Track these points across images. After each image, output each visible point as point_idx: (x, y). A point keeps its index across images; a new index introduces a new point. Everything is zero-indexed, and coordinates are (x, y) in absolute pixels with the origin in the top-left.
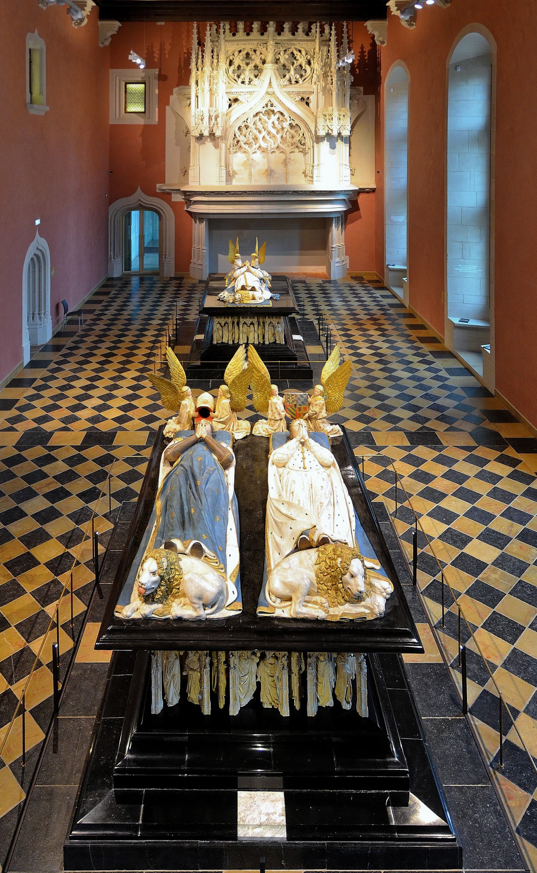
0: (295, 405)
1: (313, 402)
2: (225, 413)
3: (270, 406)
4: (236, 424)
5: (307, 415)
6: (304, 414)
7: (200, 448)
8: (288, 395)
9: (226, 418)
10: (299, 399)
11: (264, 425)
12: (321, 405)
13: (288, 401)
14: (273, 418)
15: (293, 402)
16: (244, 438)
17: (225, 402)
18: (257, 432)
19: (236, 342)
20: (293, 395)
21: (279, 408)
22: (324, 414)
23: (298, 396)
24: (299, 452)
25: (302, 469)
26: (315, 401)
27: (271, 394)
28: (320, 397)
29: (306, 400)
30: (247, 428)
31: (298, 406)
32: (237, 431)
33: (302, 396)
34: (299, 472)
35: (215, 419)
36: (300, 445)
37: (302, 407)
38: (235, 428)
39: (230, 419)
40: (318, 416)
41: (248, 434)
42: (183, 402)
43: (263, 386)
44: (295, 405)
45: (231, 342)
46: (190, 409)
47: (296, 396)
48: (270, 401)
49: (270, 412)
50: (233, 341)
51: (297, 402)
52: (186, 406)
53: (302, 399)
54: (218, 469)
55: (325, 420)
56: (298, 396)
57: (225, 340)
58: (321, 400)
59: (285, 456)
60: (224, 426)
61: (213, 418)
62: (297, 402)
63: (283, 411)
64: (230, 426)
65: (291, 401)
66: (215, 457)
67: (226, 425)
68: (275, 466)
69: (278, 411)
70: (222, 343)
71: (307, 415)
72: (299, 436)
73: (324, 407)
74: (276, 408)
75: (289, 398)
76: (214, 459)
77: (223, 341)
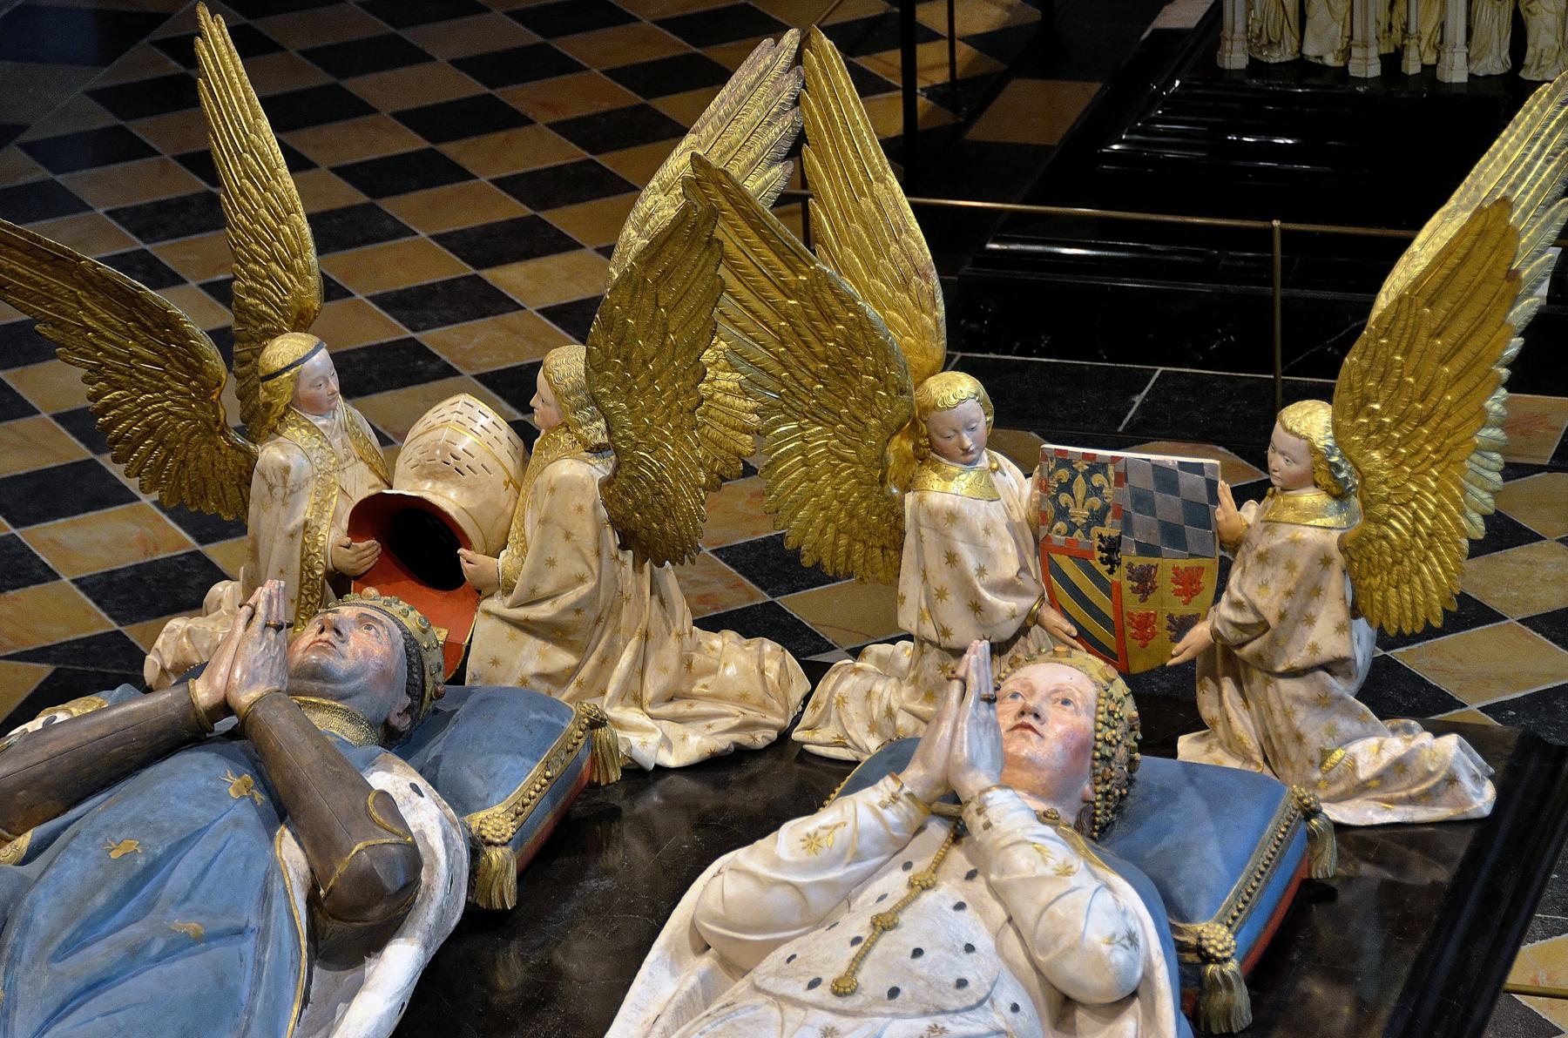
0: (1112, 548)
1: (1255, 536)
2: (569, 565)
3: (910, 540)
4: (669, 654)
5: (1199, 634)
6: (1182, 626)
7: (204, 785)
8: (1065, 462)
9: (569, 598)
10: (1142, 501)
11: (879, 687)
12: (1302, 562)
13: (1063, 513)
14: (930, 631)
15: (1098, 518)
16: (711, 766)
17: (576, 473)
18: (827, 733)
19: (1412, 67)
20: (1097, 466)
21: (970, 561)
22: (1328, 632)
23: (1135, 480)
24: (894, 882)
25: (822, 994)
26: (1269, 524)
27: (931, 444)
28: (1309, 497)
29: (1201, 513)
30: (756, 689)
31: (1130, 556)
32: (668, 709)
33: (1166, 479)
34: (794, 1014)
35: (494, 604)
36: (938, 832)
37: (1168, 564)
38: (653, 685)
39: (615, 610)
40: (1274, 642)
41: (761, 738)
42: (270, 454)
43: (842, 371)
44: (1112, 548)
45: (1367, 66)
46: (320, 508)
47: (1121, 478)
48: (910, 499)
49: (910, 586)
50: (1392, 62)
51: (1127, 527)
52: (285, 485)
53: (1169, 507)
54: (263, 934)
55: (1338, 686)
56: (1135, 480)
57: (1322, 46)
58: (1311, 523)
59: (780, 897)
60: (562, 659)
61: (479, 593)
62: (1127, 527)
63: (1008, 588)
64: (607, 662)
65: (1080, 514)
66: (290, 852)
67: (582, 651)
68: (705, 962)
69: (966, 585)
70: (1303, 67)
71: (1199, 634)
72: (926, 764)
73: (1336, 585)
74: (952, 559)
75: (1066, 487)
76: (275, 869)
77: (1310, 50)
